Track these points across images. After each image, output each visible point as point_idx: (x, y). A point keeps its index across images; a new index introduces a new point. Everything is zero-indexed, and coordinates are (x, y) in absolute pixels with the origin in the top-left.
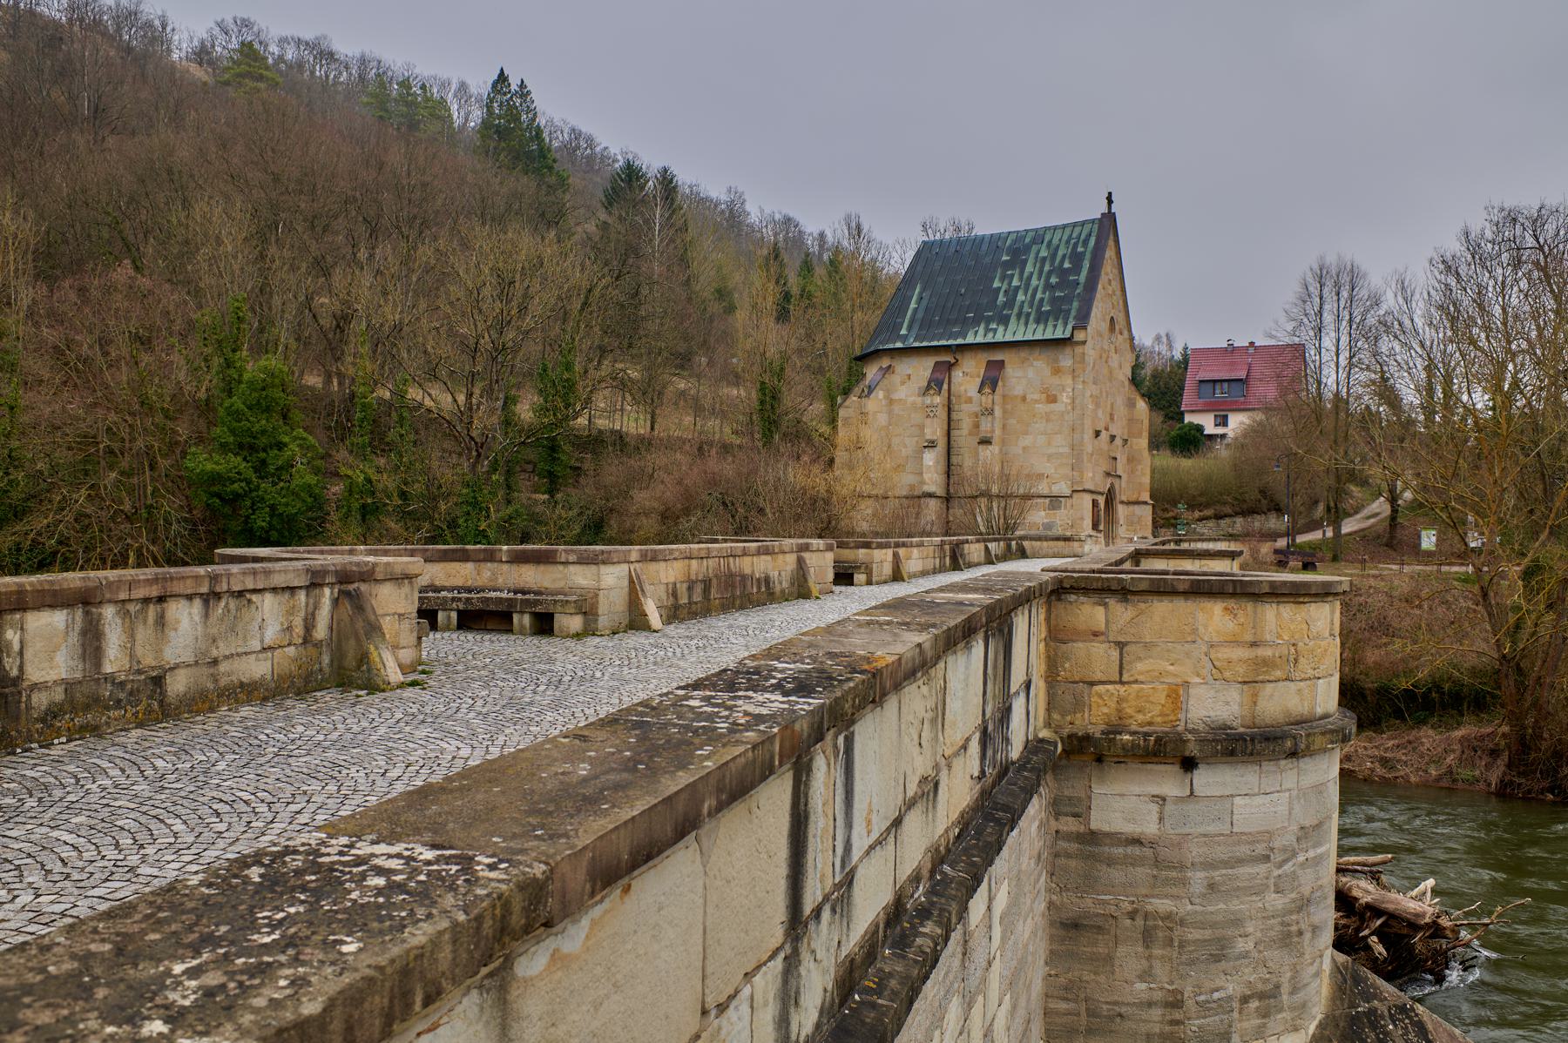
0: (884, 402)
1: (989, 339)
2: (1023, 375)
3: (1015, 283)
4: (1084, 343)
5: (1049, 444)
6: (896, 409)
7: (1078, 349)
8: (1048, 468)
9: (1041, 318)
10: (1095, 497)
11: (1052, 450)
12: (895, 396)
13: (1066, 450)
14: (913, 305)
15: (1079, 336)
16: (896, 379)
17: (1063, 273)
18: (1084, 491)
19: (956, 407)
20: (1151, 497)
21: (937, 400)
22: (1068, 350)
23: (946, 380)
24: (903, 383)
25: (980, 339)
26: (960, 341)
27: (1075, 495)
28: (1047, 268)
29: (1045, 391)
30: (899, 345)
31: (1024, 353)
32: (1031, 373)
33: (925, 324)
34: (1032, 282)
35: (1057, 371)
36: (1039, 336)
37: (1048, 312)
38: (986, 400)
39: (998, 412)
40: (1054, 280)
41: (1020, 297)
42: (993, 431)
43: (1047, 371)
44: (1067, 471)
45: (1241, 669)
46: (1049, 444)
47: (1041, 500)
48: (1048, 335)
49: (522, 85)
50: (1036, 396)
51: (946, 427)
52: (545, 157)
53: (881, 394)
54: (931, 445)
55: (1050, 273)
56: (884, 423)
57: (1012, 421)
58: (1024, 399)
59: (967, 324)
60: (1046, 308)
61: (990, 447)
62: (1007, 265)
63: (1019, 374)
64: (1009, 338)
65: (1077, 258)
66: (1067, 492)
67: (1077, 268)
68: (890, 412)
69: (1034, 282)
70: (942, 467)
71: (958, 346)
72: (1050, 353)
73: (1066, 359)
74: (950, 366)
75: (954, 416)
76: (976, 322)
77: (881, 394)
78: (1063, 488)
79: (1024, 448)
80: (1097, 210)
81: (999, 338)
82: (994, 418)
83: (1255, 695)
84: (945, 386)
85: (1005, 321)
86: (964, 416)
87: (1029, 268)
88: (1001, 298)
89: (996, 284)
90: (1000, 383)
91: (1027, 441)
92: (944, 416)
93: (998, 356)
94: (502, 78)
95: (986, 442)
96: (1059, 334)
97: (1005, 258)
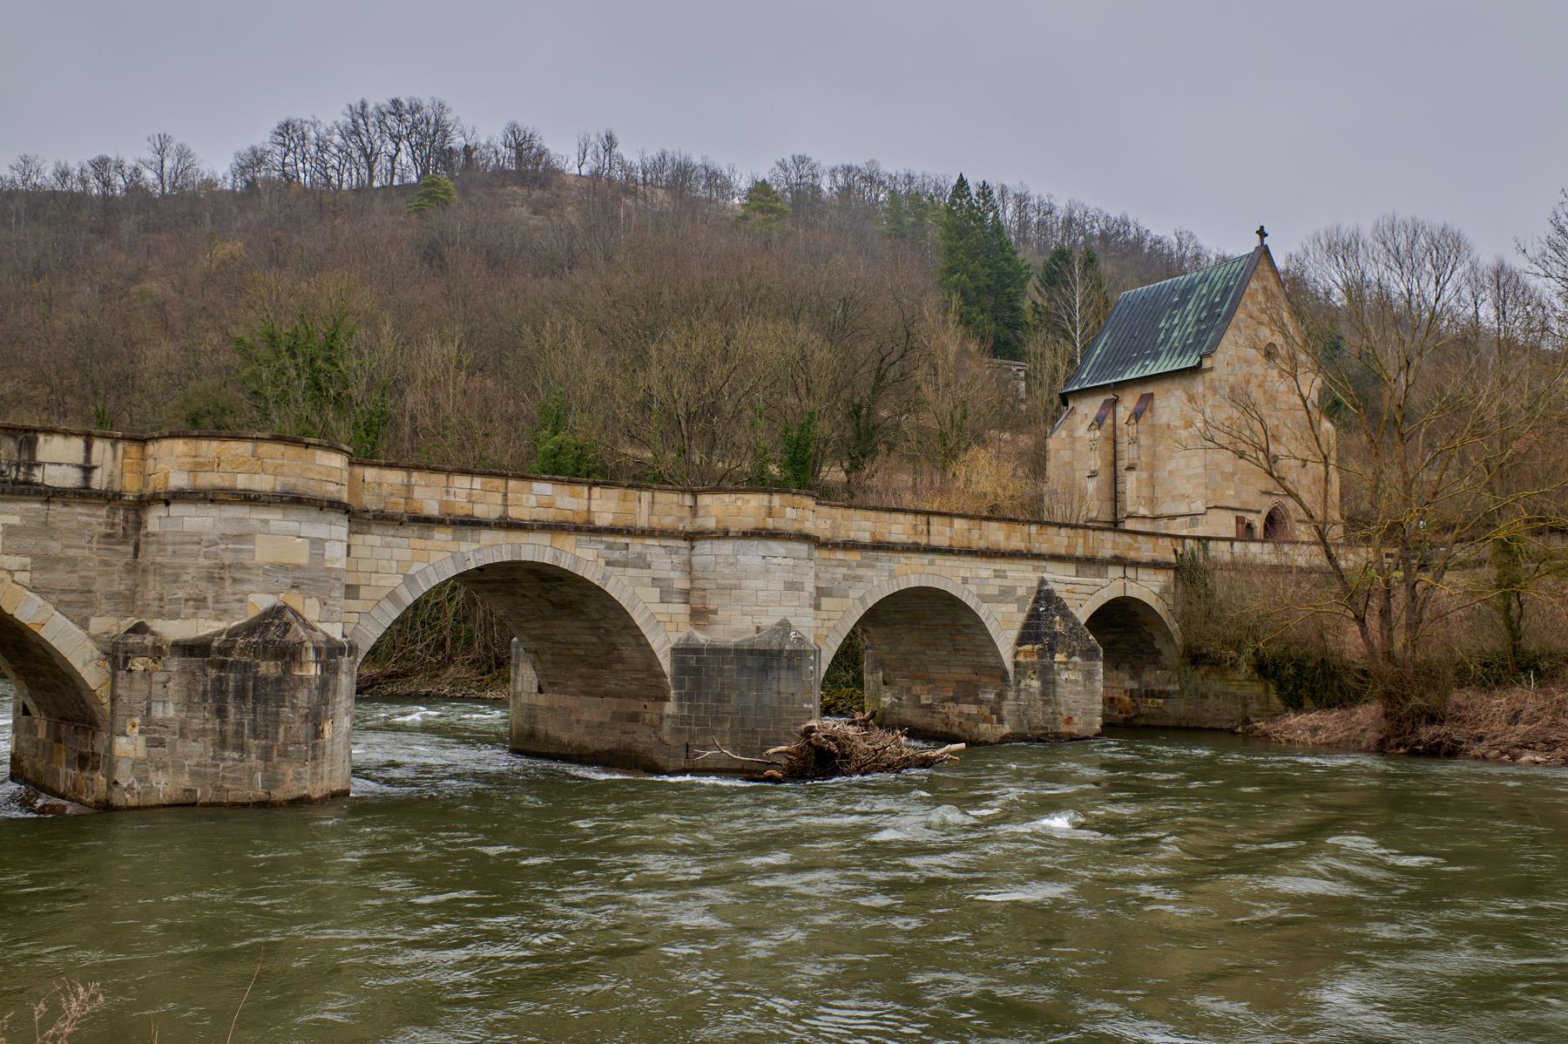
0: (1067, 441)
1: (1139, 375)
2: (1170, 404)
3: (1175, 322)
4: (1211, 369)
5: (1188, 466)
6: (1078, 445)
7: (1208, 376)
8: (1188, 489)
9: (1183, 352)
10: (1240, 514)
11: (1190, 472)
12: (1077, 434)
13: (1200, 470)
14: (1098, 352)
15: (1207, 364)
16: (1078, 418)
17: (1213, 306)
18: (1216, 507)
19: (1119, 440)
20: (1342, 516)
21: (1098, 433)
22: (1199, 378)
23: (1110, 415)
24: (1082, 422)
25: (1133, 376)
26: (1119, 379)
27: (1209, 512)
28: (1203, 304)
29: (1183, 417)
30: (1076, 388)
31: (1167, 385)
32: (1173, 402)
33: (1101, 368)
34: (1183, 324)
35: (1191, 399)
36: (1175, 368)
37: (1191, 345)
38: (1132, 430)
39: (1144, 440)
40: (1204, 314)
41: (1175, 334)
42: (1139, 458)
43: (1185, 399)
44: (1202, 490)
45: (188, 466)
46: (1188, 466)
47: (1183, 519)
48: (1182, 366)
49: (984, 186)
50: (1178, 423)
51: (1111, 458)
52: (1003, 250)
53: (1064, 434)
54: (1093, 475)
55: (1204, 307)
56: (1067, 459)
57: (1160, 448)
58: (1168, 426)
59: (1130, 362)
60: (1190, 341)
61: (1134, 473)
62: (1176, 306)
63: (1164, 404)
64: (1154, 372)
65: (1227, 289)
66: (1202, 510)
67: (1223, 299)
68: (1073, 449)
69: (1189, 318)
70: (1107, 492)
71: (1115, 383)
72: (1185, 382)
73: (1199, 386)
74: (1115, 402)
75: (1119, 448)
76: (1136, 361)
77: (1064, 434)
78: (1199, 507)
79: (1170, 472)
80: (1250, 245)
81: (1147, 373)
82: (1139, 446)
83: (195, 477)
84: (1109, 421)
85: (1156, 356)
86: (1123, 446)
87: (1190, 307)
88: (1162, 337)
89: (1162, 325)
90: (1148, 414)
91: (1171, 465)
92: (1109, 448)
93: (1149, 389)
94: (962, 182)
95: (1131, 468)
96: (1190, 364)
97: (1176, 299)
